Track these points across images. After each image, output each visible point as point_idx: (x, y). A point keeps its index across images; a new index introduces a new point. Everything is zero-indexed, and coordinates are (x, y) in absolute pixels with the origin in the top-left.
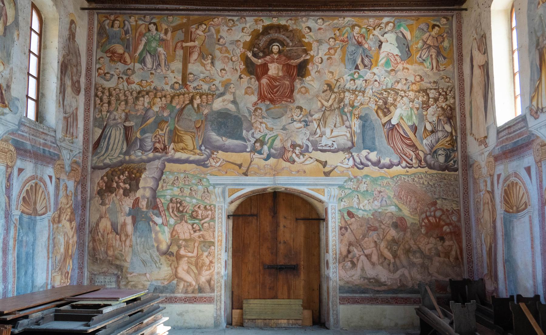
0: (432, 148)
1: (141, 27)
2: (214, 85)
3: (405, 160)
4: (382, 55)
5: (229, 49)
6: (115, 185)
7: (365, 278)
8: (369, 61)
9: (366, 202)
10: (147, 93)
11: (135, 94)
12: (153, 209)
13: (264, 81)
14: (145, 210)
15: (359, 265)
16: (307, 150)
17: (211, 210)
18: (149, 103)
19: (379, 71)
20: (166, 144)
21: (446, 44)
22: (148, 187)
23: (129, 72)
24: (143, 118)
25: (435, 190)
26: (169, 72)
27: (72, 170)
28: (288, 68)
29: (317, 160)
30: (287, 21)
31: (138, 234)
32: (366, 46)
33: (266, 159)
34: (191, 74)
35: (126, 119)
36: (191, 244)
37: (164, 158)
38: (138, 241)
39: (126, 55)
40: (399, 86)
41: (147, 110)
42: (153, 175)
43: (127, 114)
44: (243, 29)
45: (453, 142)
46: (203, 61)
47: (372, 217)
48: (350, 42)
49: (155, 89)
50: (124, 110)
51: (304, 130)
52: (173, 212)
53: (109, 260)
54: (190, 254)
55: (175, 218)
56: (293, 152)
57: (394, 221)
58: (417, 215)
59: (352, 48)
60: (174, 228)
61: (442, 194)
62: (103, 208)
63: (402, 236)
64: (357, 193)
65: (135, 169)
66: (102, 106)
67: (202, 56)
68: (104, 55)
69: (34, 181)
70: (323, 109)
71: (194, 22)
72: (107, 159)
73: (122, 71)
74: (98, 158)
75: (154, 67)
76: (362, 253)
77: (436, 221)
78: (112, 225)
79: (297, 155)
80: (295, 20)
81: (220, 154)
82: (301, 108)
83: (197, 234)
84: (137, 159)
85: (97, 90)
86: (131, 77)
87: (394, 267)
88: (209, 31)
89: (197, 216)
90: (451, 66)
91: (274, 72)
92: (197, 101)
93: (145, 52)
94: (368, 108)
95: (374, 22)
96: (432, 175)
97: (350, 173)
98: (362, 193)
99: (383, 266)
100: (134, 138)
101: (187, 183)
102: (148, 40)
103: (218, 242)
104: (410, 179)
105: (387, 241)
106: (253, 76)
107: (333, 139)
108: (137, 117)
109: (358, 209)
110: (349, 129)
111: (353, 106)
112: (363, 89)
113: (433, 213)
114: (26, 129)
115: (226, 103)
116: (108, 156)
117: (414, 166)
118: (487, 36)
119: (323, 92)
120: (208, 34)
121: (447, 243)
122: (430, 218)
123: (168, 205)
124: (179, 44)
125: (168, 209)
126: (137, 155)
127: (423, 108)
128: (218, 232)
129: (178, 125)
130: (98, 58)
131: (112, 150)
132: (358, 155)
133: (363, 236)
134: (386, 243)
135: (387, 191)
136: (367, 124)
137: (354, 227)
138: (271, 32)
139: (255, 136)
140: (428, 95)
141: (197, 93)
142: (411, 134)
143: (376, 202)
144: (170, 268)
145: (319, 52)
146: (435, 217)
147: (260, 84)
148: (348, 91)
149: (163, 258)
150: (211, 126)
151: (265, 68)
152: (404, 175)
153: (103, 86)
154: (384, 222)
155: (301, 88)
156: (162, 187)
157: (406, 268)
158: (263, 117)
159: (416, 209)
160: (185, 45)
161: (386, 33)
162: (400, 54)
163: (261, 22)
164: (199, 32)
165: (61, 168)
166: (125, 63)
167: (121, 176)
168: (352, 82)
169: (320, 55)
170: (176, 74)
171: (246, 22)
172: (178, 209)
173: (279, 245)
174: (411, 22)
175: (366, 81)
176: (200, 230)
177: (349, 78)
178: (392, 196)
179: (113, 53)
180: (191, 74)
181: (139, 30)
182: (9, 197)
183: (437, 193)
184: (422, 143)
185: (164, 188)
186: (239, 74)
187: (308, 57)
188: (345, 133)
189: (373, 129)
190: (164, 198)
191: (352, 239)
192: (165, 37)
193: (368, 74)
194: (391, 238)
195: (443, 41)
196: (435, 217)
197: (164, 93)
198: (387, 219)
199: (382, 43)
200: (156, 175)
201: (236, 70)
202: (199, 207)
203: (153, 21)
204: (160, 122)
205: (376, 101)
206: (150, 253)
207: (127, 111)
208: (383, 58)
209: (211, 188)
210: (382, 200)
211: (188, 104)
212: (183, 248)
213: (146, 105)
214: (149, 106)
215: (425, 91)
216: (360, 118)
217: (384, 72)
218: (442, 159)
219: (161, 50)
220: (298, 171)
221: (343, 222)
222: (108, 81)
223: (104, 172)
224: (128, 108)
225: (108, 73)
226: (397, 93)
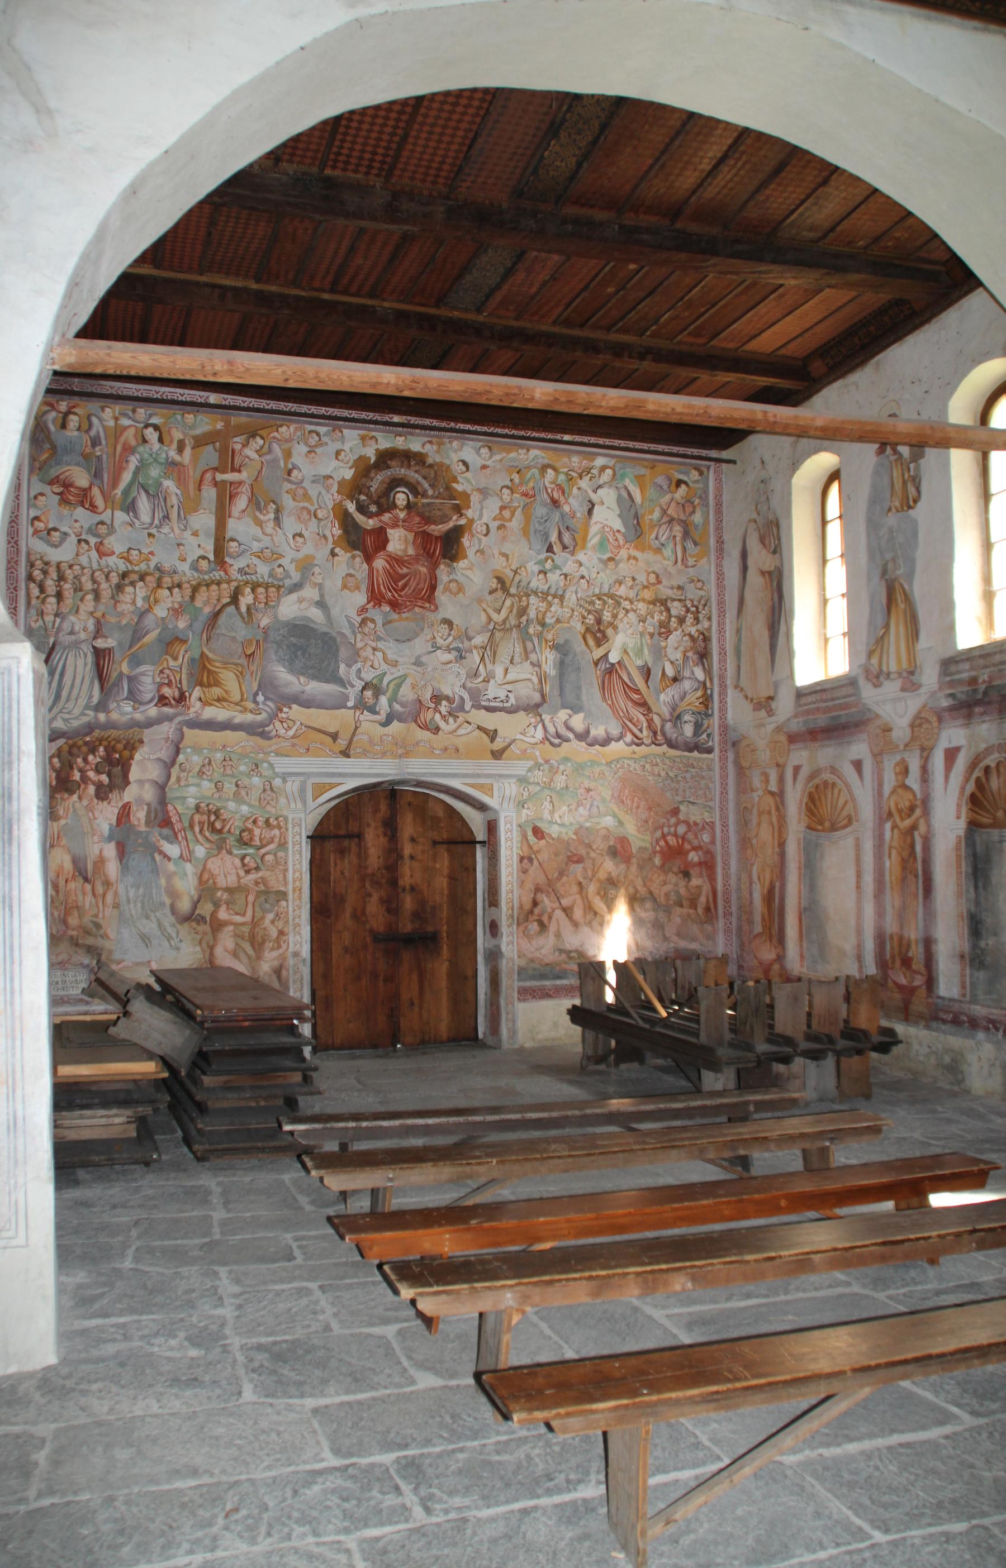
0: (674, 710)
1: (126, 434)
2: (280, 566)
3: (631, 731)
4: (594, 529)
5: (310, 493)
6: (77, 776)
7: (561, 951)
8: (569, 537)
9: (565, 808)
10: (142, 578)
11: (115, 579)
12: (161, 826)
13: (380, 563)
14: (143, 828)
15: (552, 928)
16: (461, 708)
17: (279, 827)
18: (146, 599)
19: (588, 558)
20: (185, 688)
21: (697, 518)
22: (148, 780)
23: (103, 530)
24: (135, 632)
26: (187, 534)
28: (424, 540)
29: (479, 728)
30: (423, 445)
31: (130, 879)
32: (566, 508)
33: (386, 724)
34: (233, 540)
35: (98, 633)
36: (240, 898)
37: (180, 718)
38: (132, 893)
40: (622, 591)
41: (142, 614)
42: (159, 755)
43: (98, 623)
44: (338, 453)
45: (706, 700)
46: (258, 514)
48: (538, 497)
49: (158, 568)
50: (91, 613)
51: (455, 667)
52: (201, 831)
53: (72, 937)
54: (238, 919)
55: (207, 845)
56: (436, 710)
57: (611, 843)
59: (540, 511)
60: (205, 866)
61: (688, 793)
64: (547, 792)
65: (119, 741)
66: (43, 602)
67: (255, 503)
68: (47, 489)
70: (491, 627)
71: (239, 430)
73: (86, 526)
75: (157, 522)
76: (557, 904)
78: (75, 861)
79: (443, 717)
80: (440, 444)
81: (296, 711)
82: (449, 623)
83: (253, 876)
84: (125, 719)
85: (32, 565)
86: (106, 542)
88: (270, 451)
89: (251, 839)
90: (705, 559)
91: (398, 547)
92: (246, 599)
93: (135, 488)
94: (570, 628)
95: (580, 463)
96: (673, 759)
97: (538, 753)
100: (114, 675)
101: (229, 772)
102: (141, 461)
103: (294, 891)
104: (637, 766)
105: (600, 881)
106: (357, 552)
107: (509, 687)
108: (121, 629)
109: (551, 822)
110: (537, 669)
111: (543, 625)
112: (560, 592)
113: (672, 829)
115: (304, 605)
116: (60, 712)
117: (645, 741)
118: (783, 523)
119: (491, 593)
120: (268, 457)
121: (695, 882)
122: (669, 838)
123: (192, 818)
124: (208, 476)
125: (191, 826)
126: (123, 711)
127: (660, 634)
128: (294, 872)
129: (209, 650)
130: (32, 495)
131: (68, 700)
132: (552, 720)
136: (567, 660)
137: (544, 856)
138: (392, 463)
139: (363, 675)
140: (668, 610)
141: (247, 582)
142: (640, 682)
143: (581, 809)
144: (198, 948)
145: (482, 513)
146: (676, 835)
147: (371, 570)
148: (535, 593)
149: (185, 929)
150: (276, 652)
151: (380, 538)
152: (629, 759)
153: (46, 559)
155: (450, 581)
156: (179, 779)
158: (379, 639)
159: (646, 822)
160: (220, 477)
161: (600, 487)
162: (623, 530)
163: (373, 442)
164: (250, 452)
166: (93, 508)
167: (91, 757)
168: (541, 576)
169: (485, 520)
170: (202, 539)
171: (343, 439)
172: (212, 825)
173: (402, 895)
174: (643, 471)
175: (566, 576)
176: (257, 869)
177: (536, 568)
178: (608, 798)
179: (67, 485)
180: (233, 540)
181: (122, 439)
183: (681, 792)
184: (658, 699)
185: (183, 783)
186: (330, 546)
187: (463, 522)
188: (529, 676)
189: (578, 669)
190: (183, 804)
191: (541, 879)
192: (177, 458)
193: (570, 563)
194: (606, 876)
195: (694, 512)
196: (676, 835)
197: (176, 578)
199: (593, 505)
200: (165, 754)
201: (325, 537)
202: (255, 822)
203: (154, 420)
204: (170, 642)
205: (584, 617)
206: (158, 920)
207: (99, 614)
208: (595, 535)
209: (277, 782)
211: (228, 604)
212: (224, 907)
213: (140, 603)
214: (146, 606)
215: (663, 603)
216: (555, 647)
217: (595, 561)
218: (688, 730)
219: (169, 484)
220: (446, 749)
221: (526, 848)
222: (56, 546)
224: (102, 608)
225: (55, 529)
226: (619, 604)
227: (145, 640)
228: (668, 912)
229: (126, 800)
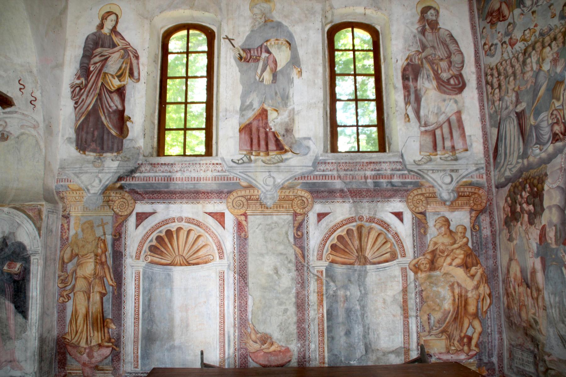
6: (518, 209)
14: (554, 246)
18: (538, 62)
22: (555, 205)
27: (459, 196)
35: (518, 102)
39: (504, 6)
41: (537, 75)
42: (558, 184)
49: (541, 34)
50: (513, 89)
53: (524, 327)
62: (512, 245)
69: (354, 224)
72: (508, 170)
74: (500, 171)
100: (528, 128)
114: (329, 167)
126: (537, 153)
153: (491, 67)
165: (427, 198)
166: (504, 18)
182: (302, 248)
197: (552, 34)
223: (507, 189)
227: (540, 94)
229: (543, 224)
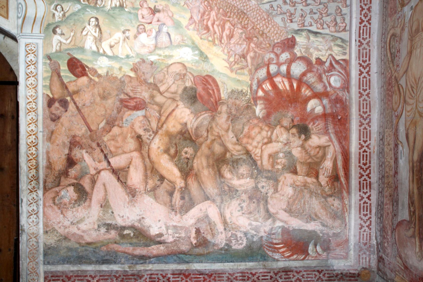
7: (109, 227)
9: (118, 35)
15: (97, 195)
25: (292, 9)
47: (132, 74)
57: (188, 84)
58: (246, 71)
61: (308, 20)
63: (206, 123)
64: (94, 13)
76: (104, 164)
77: (291, 86)
87: (183, 198)
98: (108, 13)
99: (156, 198)
109: (97, 54)
113: (284, 68)
121: (316, 140)
122: (278, 80)
133: (108, 123)
134: (166, 139)
135: (173, 9)
143: (143, 37)
146: (288, 76)
154: (162, 89)
157: (214, 201)
159: (244, 56)
178: (185, 22)
183: (297, 18)
194: (179, 127)
196: (288, 76)
198: (170, 81)
210: (159, 32)
221: (57, 88)
228: (274, 179)
